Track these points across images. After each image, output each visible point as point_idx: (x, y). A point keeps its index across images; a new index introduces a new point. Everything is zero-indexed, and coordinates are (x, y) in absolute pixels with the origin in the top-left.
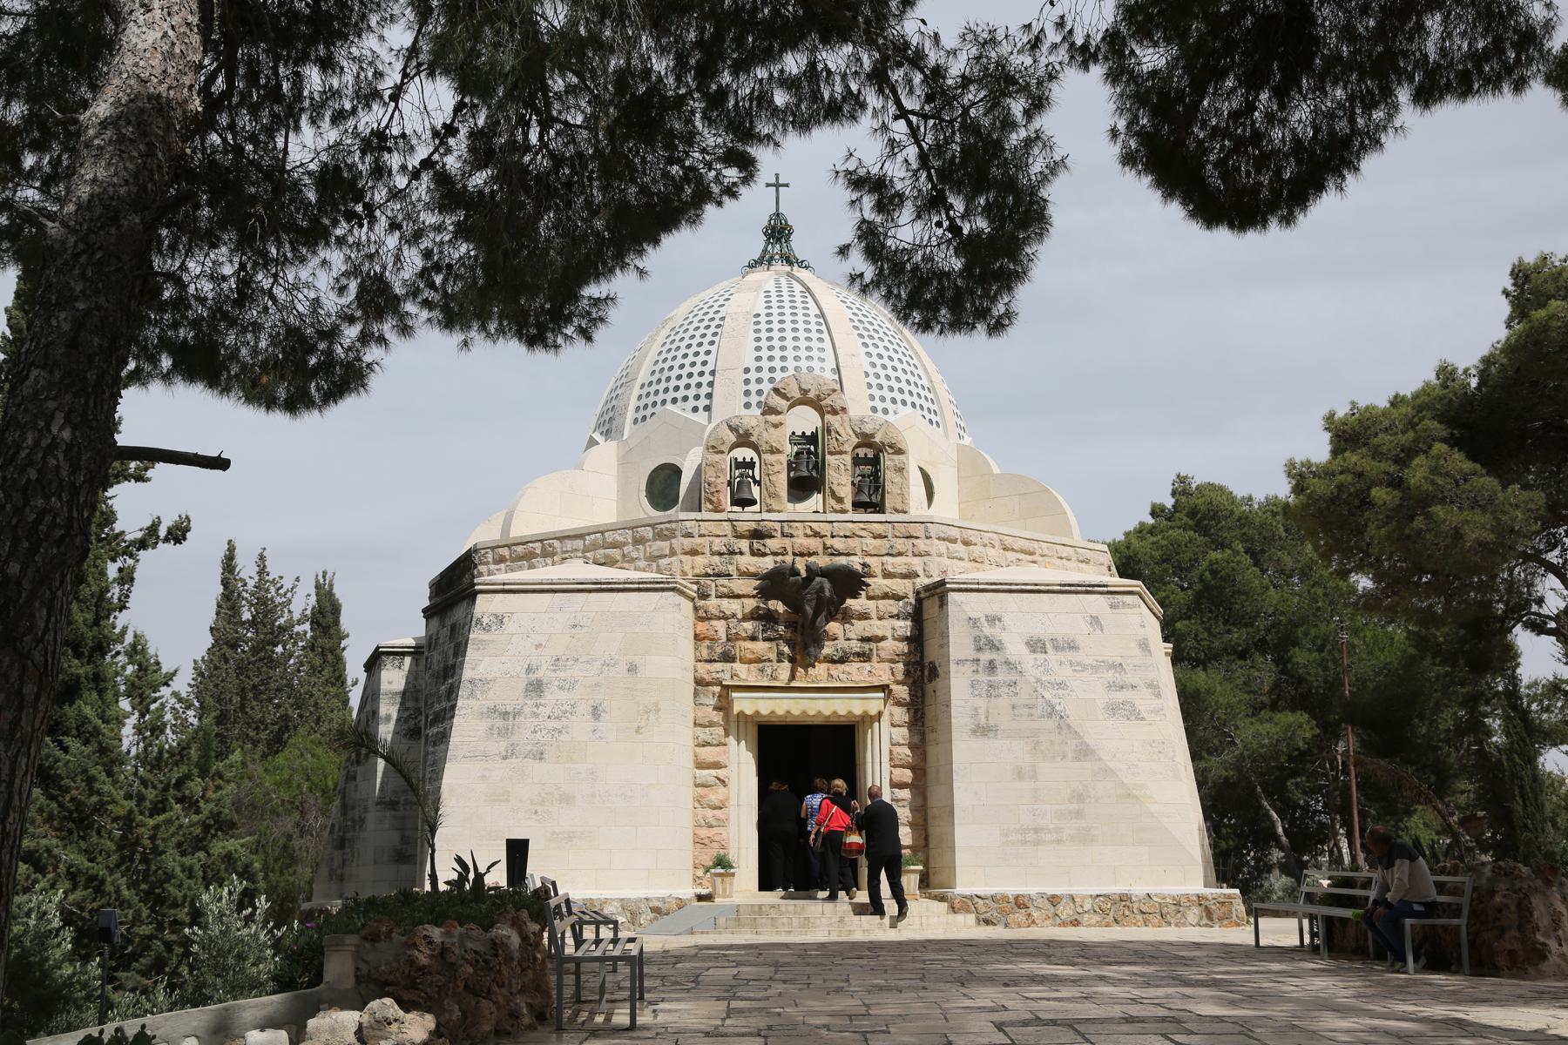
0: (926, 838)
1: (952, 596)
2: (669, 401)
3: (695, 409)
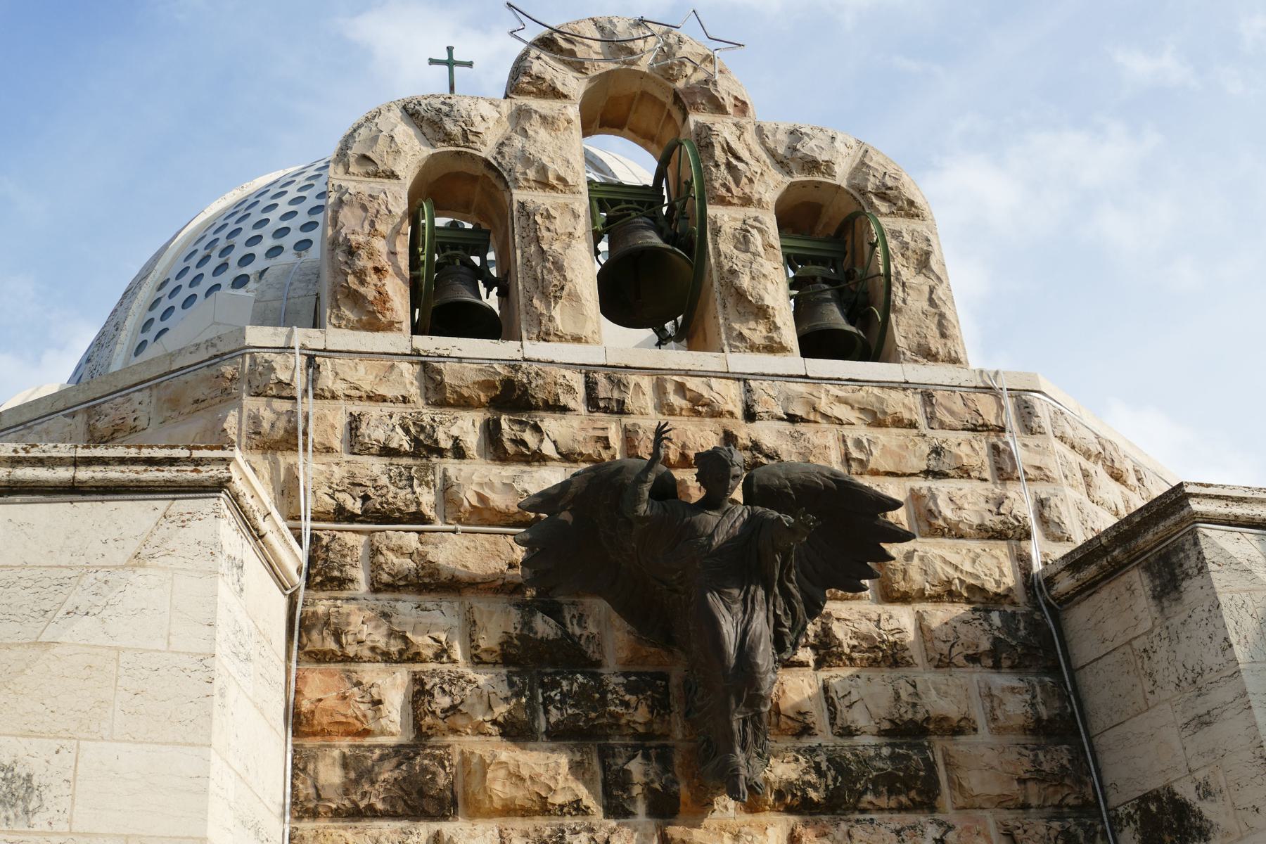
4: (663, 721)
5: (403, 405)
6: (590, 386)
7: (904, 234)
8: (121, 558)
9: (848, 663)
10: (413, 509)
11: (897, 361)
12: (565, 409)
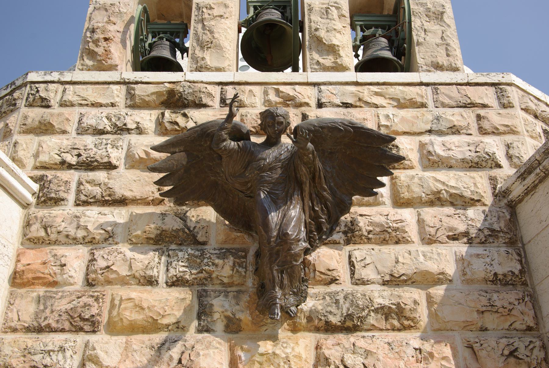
4: (241, 275)
5: (111, 108)
7: (428, 4)
9: (366, 240)
10: (106, 160)
11: (417, 71)
12: (205, 106)
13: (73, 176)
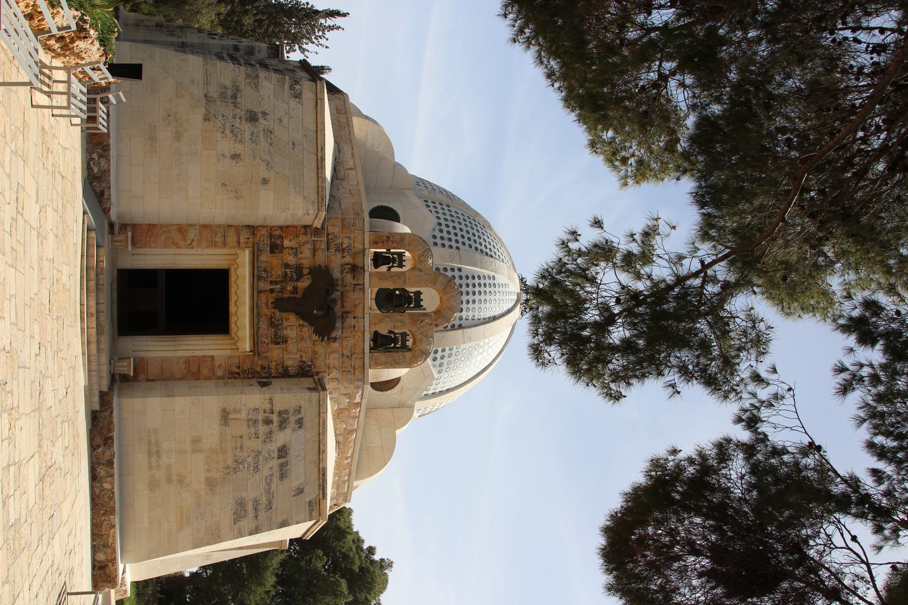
0: (153, 380)
1: (314, 395)
2: (440, 221)
3: (435, 237)
6: (360, 285)
8: (305, 195)
12: (354, 279)
13: (324, 239)
